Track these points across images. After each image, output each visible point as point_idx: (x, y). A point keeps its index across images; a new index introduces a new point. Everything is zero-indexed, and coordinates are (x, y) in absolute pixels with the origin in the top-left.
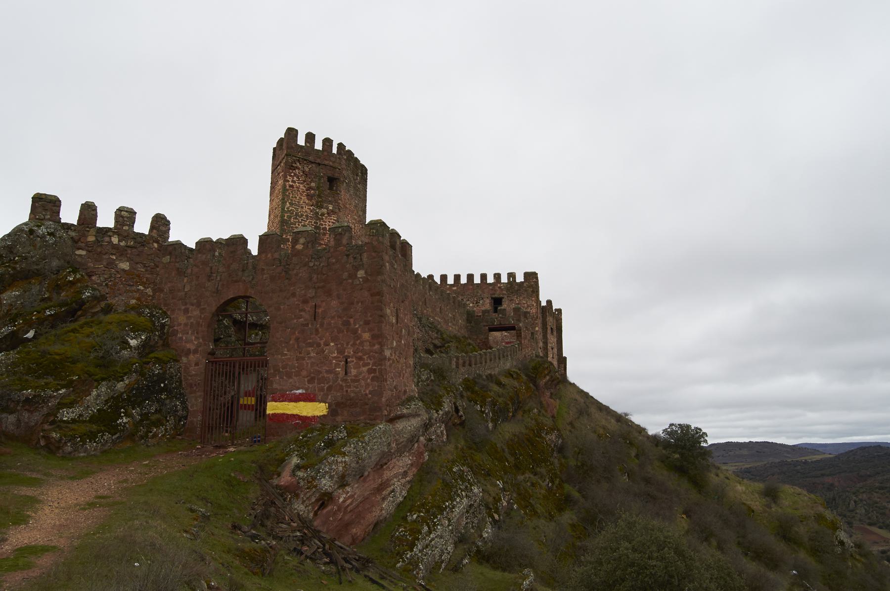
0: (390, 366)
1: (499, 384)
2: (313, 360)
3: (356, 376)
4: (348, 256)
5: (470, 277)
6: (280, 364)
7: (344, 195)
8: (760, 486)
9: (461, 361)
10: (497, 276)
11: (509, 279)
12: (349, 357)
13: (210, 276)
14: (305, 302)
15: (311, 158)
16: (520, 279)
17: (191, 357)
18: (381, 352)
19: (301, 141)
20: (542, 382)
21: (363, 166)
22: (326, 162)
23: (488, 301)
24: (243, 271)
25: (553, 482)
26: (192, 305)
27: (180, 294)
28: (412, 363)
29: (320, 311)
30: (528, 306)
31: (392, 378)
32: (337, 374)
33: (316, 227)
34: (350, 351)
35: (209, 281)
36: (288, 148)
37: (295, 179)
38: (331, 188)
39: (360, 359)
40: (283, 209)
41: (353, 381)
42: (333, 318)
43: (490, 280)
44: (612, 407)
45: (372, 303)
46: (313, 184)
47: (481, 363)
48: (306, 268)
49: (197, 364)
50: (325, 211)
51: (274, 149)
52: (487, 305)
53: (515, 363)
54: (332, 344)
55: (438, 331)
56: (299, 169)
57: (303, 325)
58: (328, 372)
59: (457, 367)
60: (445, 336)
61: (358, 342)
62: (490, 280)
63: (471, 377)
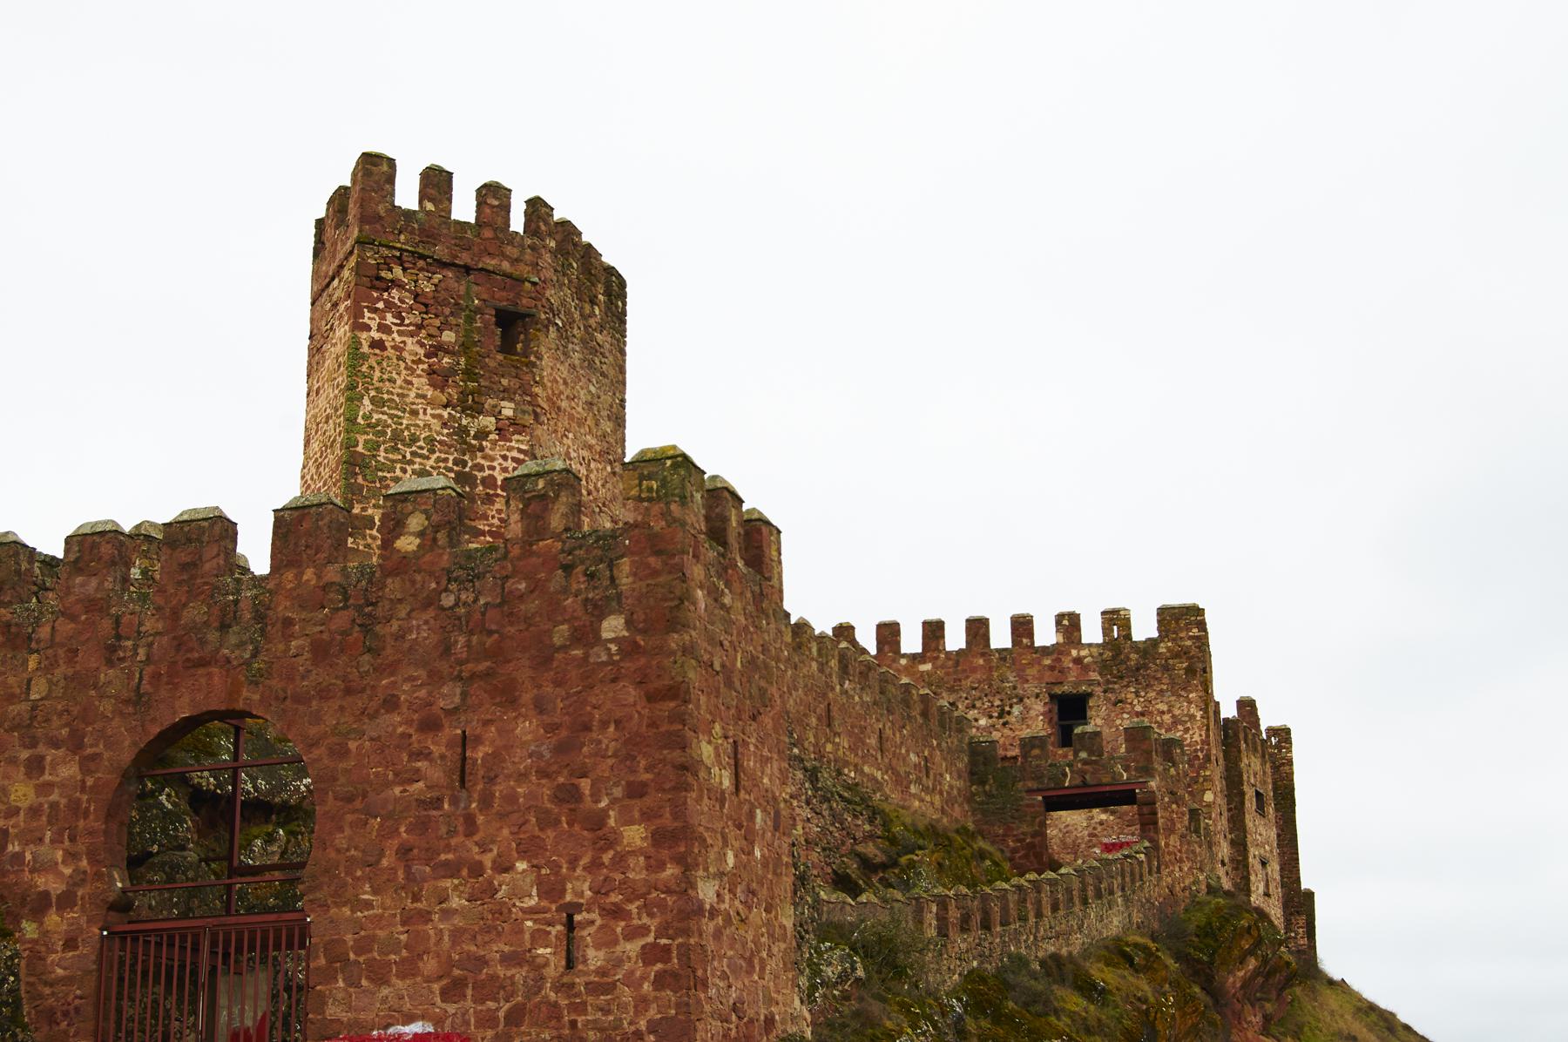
0: (718, 934)
1: (1087, 988)
2: (457, 921)
3: (602, 972)
4: (568, 569)
5: (977, 628)
6: (349, 938)
7: (552, 365)
9: (954, 914)
10: (1069, 624)
11: (1106, 631)
12: (578, 908)
13: (113, 649)
14: (430, 725)
15: (440, 251)
16: (1144, 628)
17: (53, 919)
18: (686, 886)
19: (407, 195)
20: (1234, 979)
21: (611, 271)
22: (491, 263)
23: (1038, 707)
24: (224, 627)
26: (55, 743)
27: (13, 709)
28: (789, 923)
29: (479, 754)
30: (1176, 721)
31: (724, 977)
32: (538, 967)
33: (462, 478)
34: (580, 888)
35: (110, 663)
36: (363, 220)
37: (390, 319)
38: (507, 347)
39: (616, 913)
40: (352, 420)
41: (594, 989)
42: (522, 777)
43: (1045, 635)
45: (653, 724)
46: (448, 337)
47: (1023, 919)
48: (431, 613)
49: (70, 943)
50: (488, 422)
51: (320, 224)
52: (1035, 720)
53: (1137, 918)
54: (521, 866)
55: (874, 813)
56: (401, 286)
57: (422, 803)
58: (508, 960)
59: (943, 932)
60: (897, 829)
61: (607, 857)
62: (1045, 635)
63: (989, 968)
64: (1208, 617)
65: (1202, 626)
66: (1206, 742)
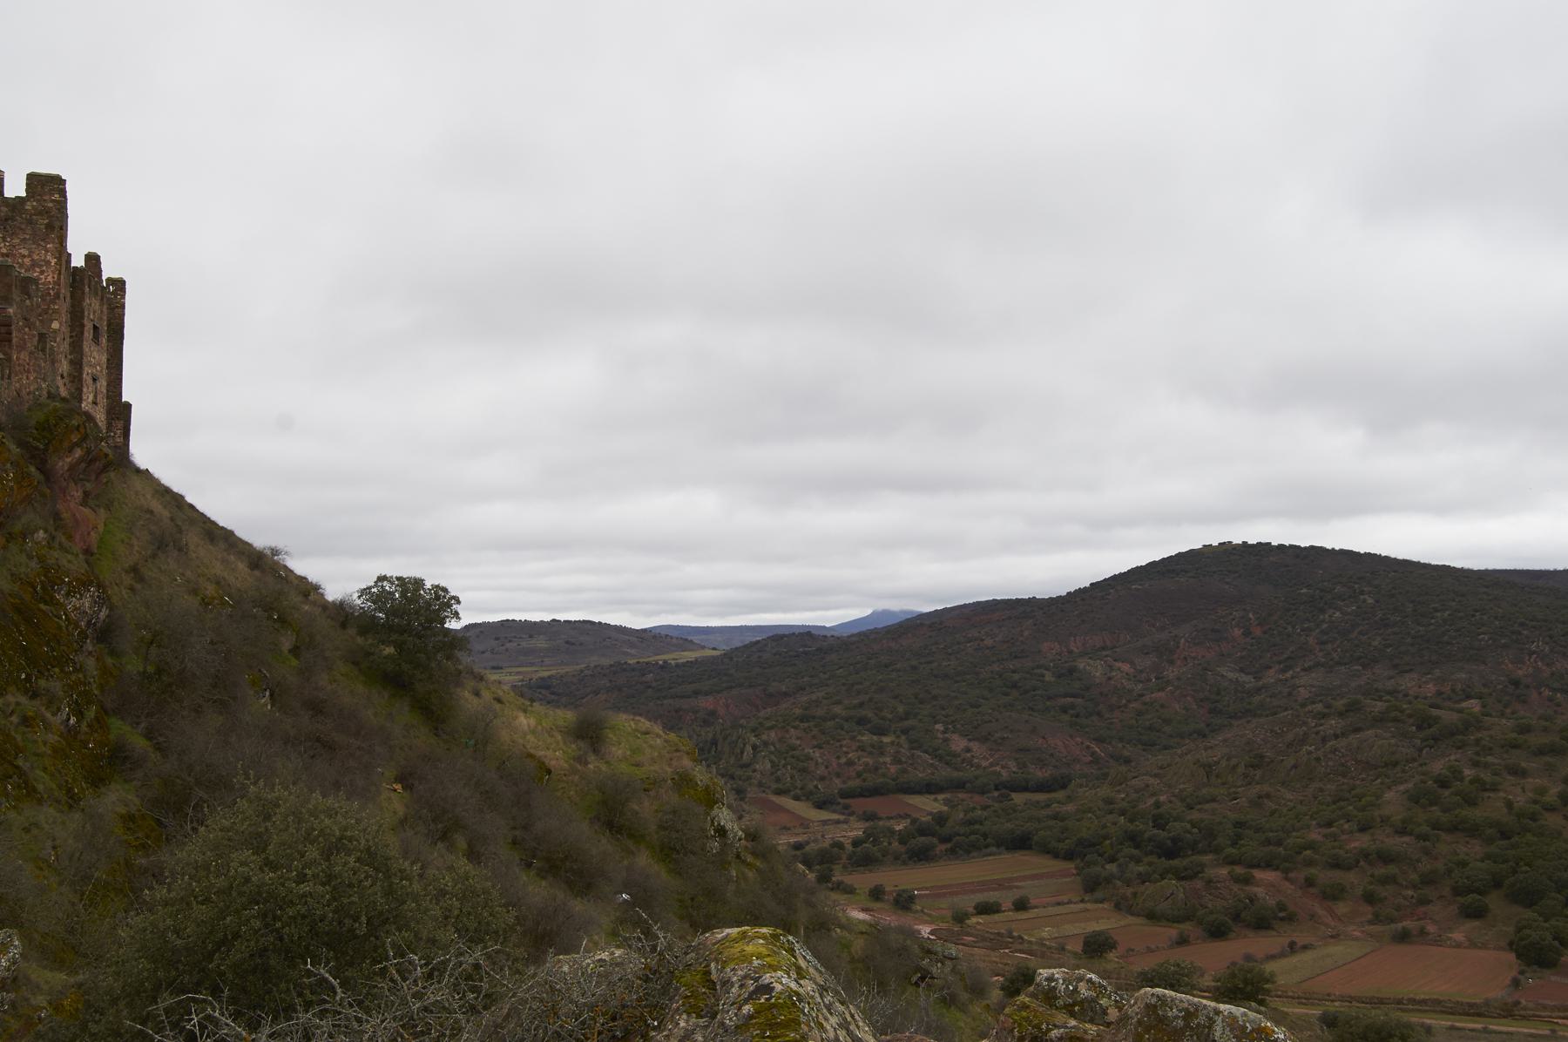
8: (567, 716)
20: (62, 464)
25: (80, 715)
30: (34, 264)
44: (241, 533)
64: (68, 187)
65: (63, 193)
66: (58, 283)
